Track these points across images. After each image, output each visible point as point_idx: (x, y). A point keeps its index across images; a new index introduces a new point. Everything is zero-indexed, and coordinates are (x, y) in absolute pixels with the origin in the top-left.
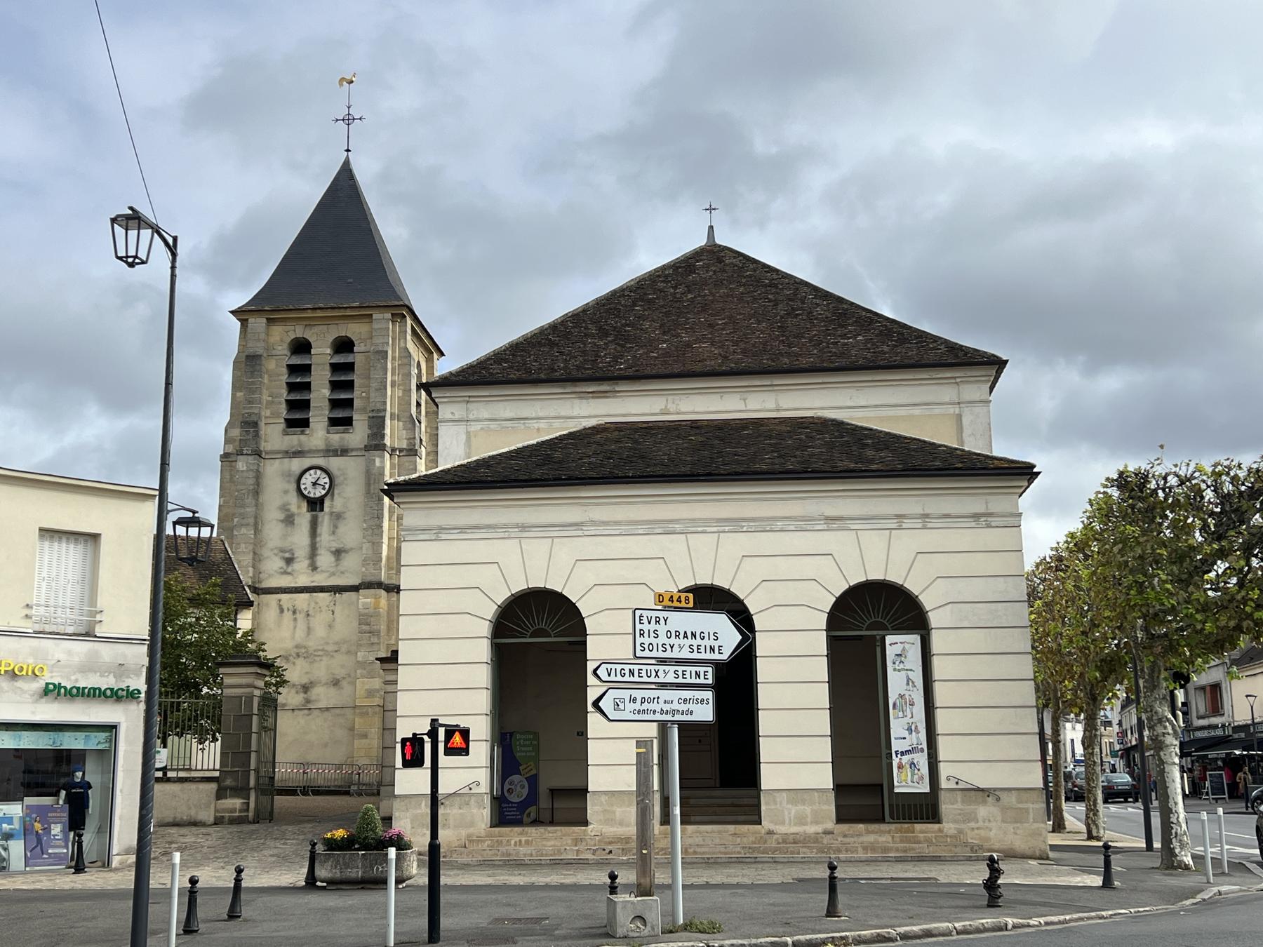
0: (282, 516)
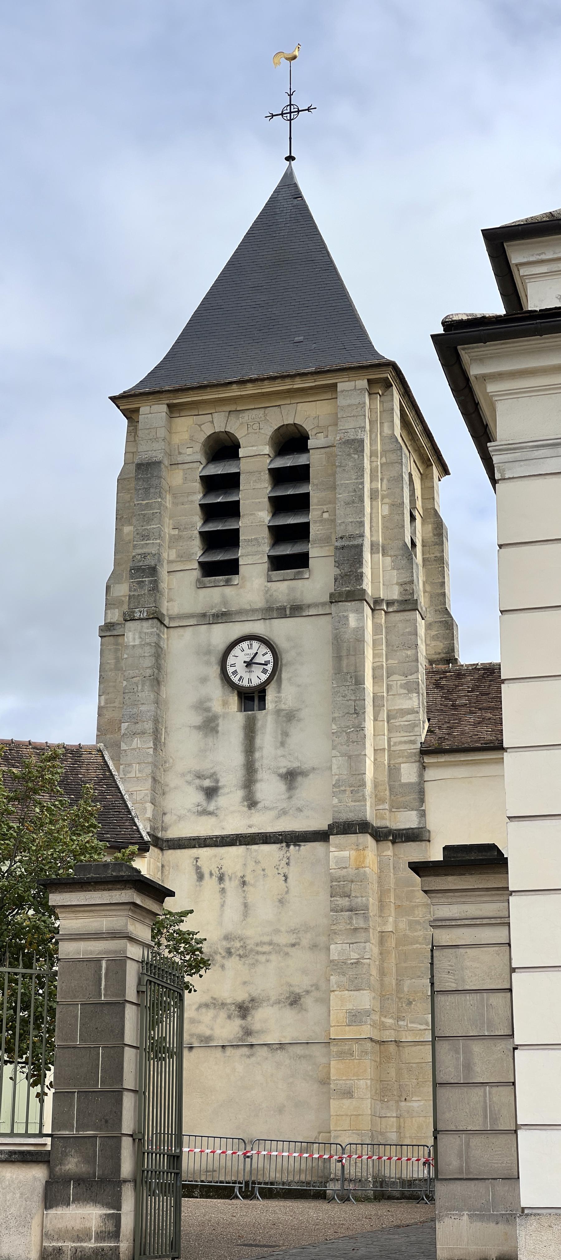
0: (197, 719)
